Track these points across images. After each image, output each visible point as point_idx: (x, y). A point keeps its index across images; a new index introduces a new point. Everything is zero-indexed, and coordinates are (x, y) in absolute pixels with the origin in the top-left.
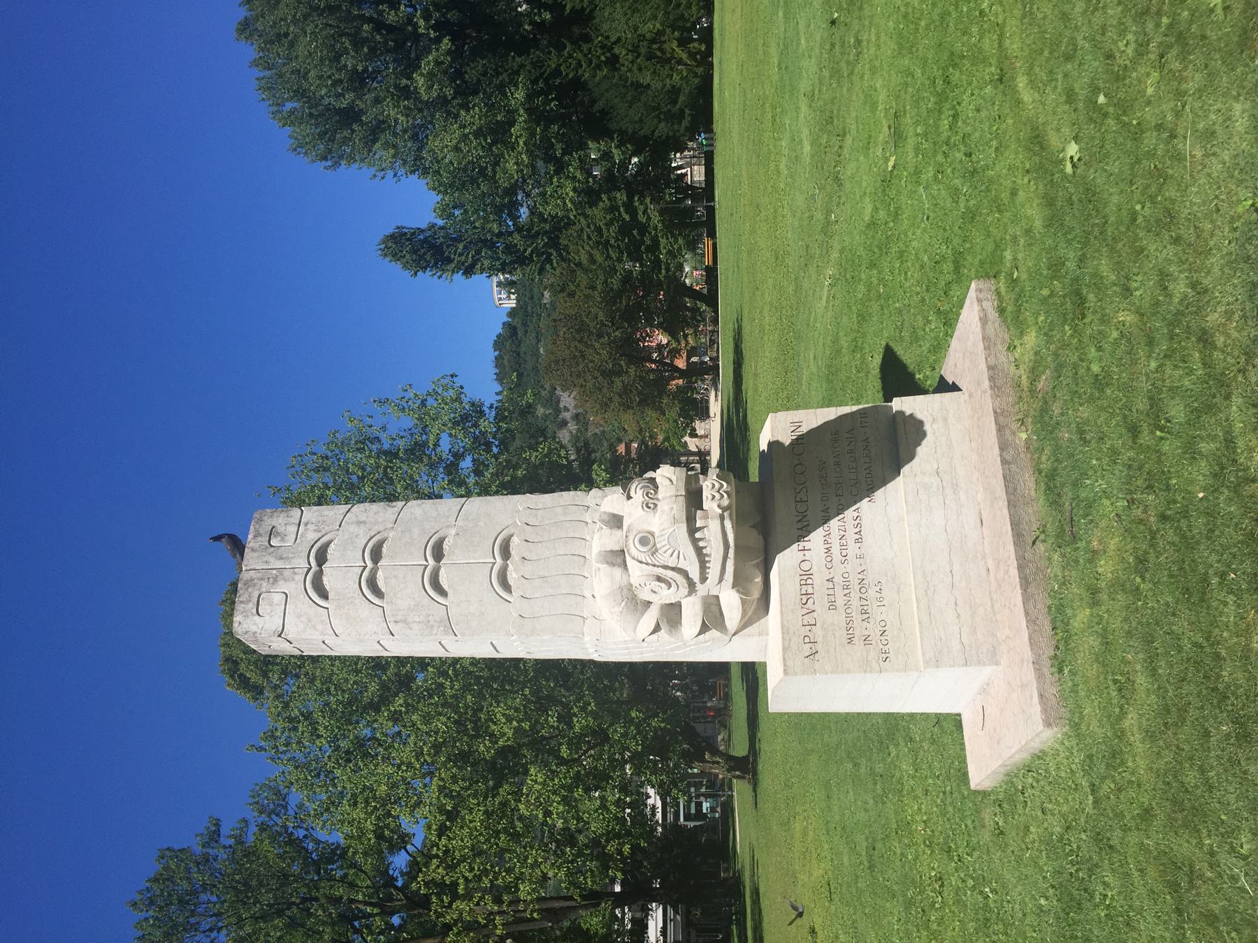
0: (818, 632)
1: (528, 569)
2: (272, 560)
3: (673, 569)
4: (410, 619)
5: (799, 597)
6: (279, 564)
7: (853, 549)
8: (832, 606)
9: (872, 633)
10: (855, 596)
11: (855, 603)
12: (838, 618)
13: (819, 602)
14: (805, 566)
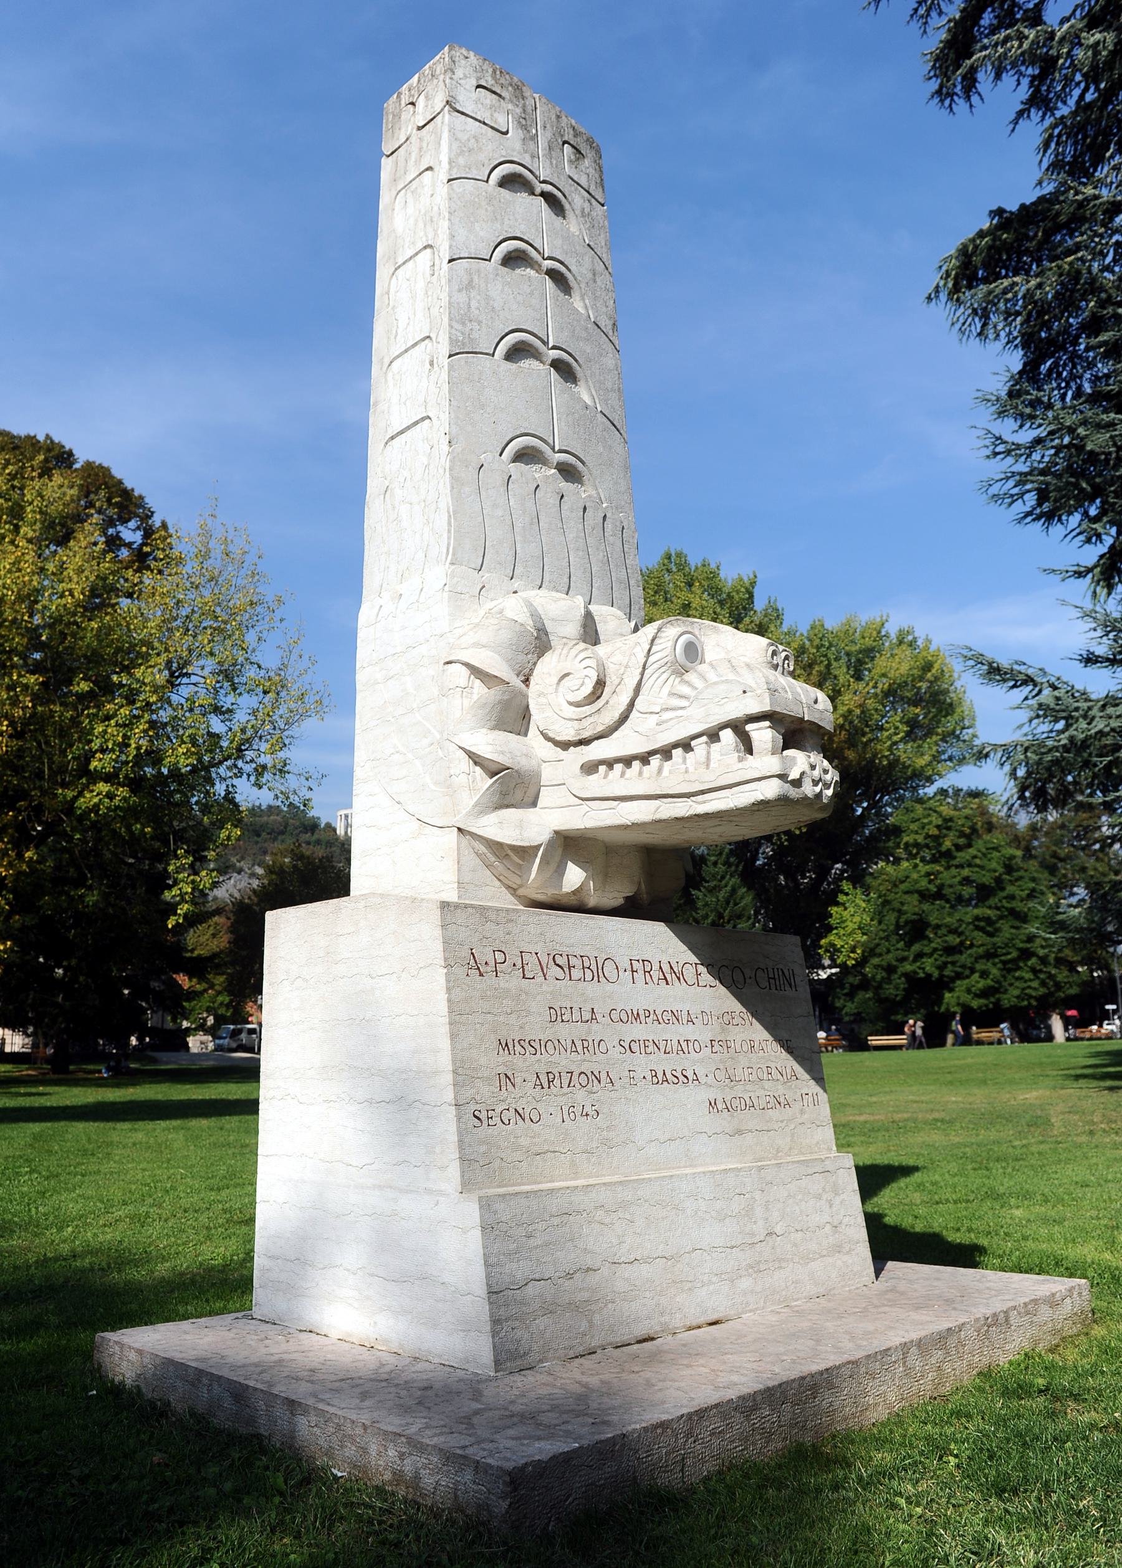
0: (511, 982)
2: (549, 134)
3: (631, 705)
4: (473, 293)
5: (565, 950)
6: (542, 142)
7: (642, 1064)
8: (557, 1015)
9: (517, 1092)
11: (564, 1061)
12: (537, 1028)
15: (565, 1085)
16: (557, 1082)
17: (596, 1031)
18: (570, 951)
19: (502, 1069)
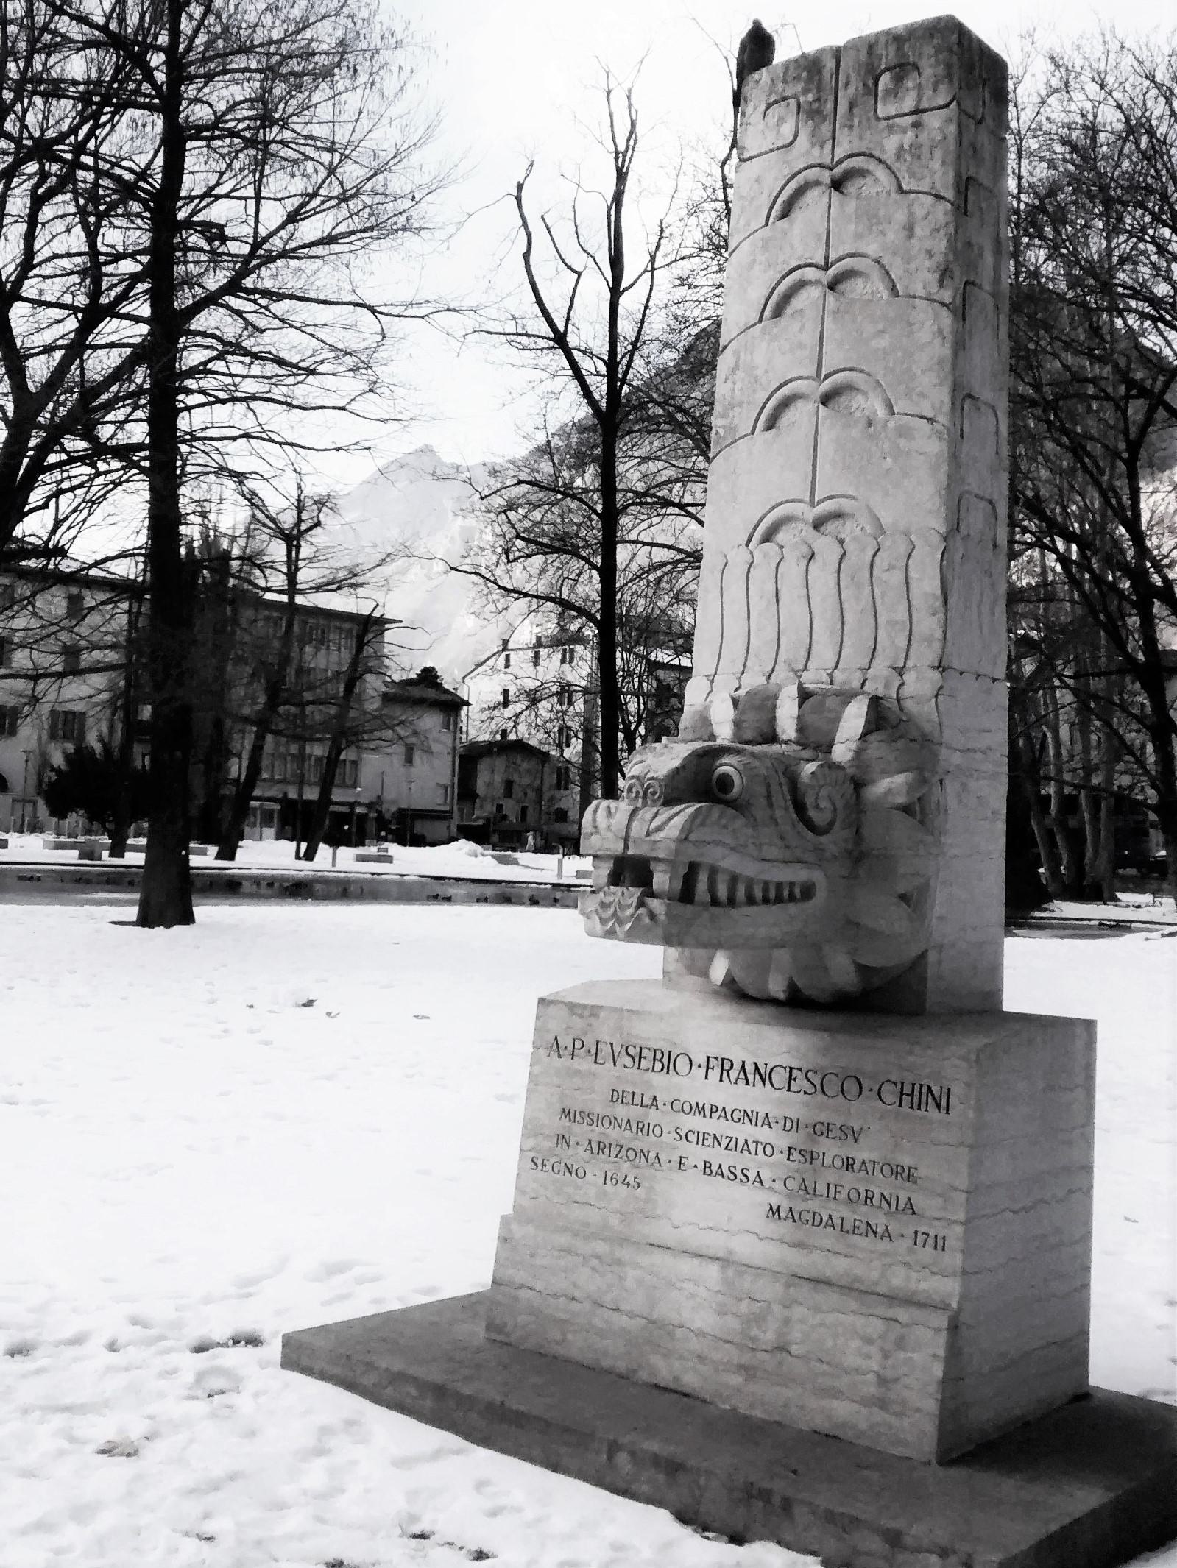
1: (793, 570)
2: (851, 90)
5: (639, 1043)
7: (696, 1154)
8: (617, 1097)
9: (570, 1152)
10: (624, 1136)
11: (614, 1134)
13: (626, 1076)
14: (682, 1064)
15: (613, 1154)
16: (606, 1151)
17: (653, 1116)
18: (644, 1043)
19: (561, 1132)
